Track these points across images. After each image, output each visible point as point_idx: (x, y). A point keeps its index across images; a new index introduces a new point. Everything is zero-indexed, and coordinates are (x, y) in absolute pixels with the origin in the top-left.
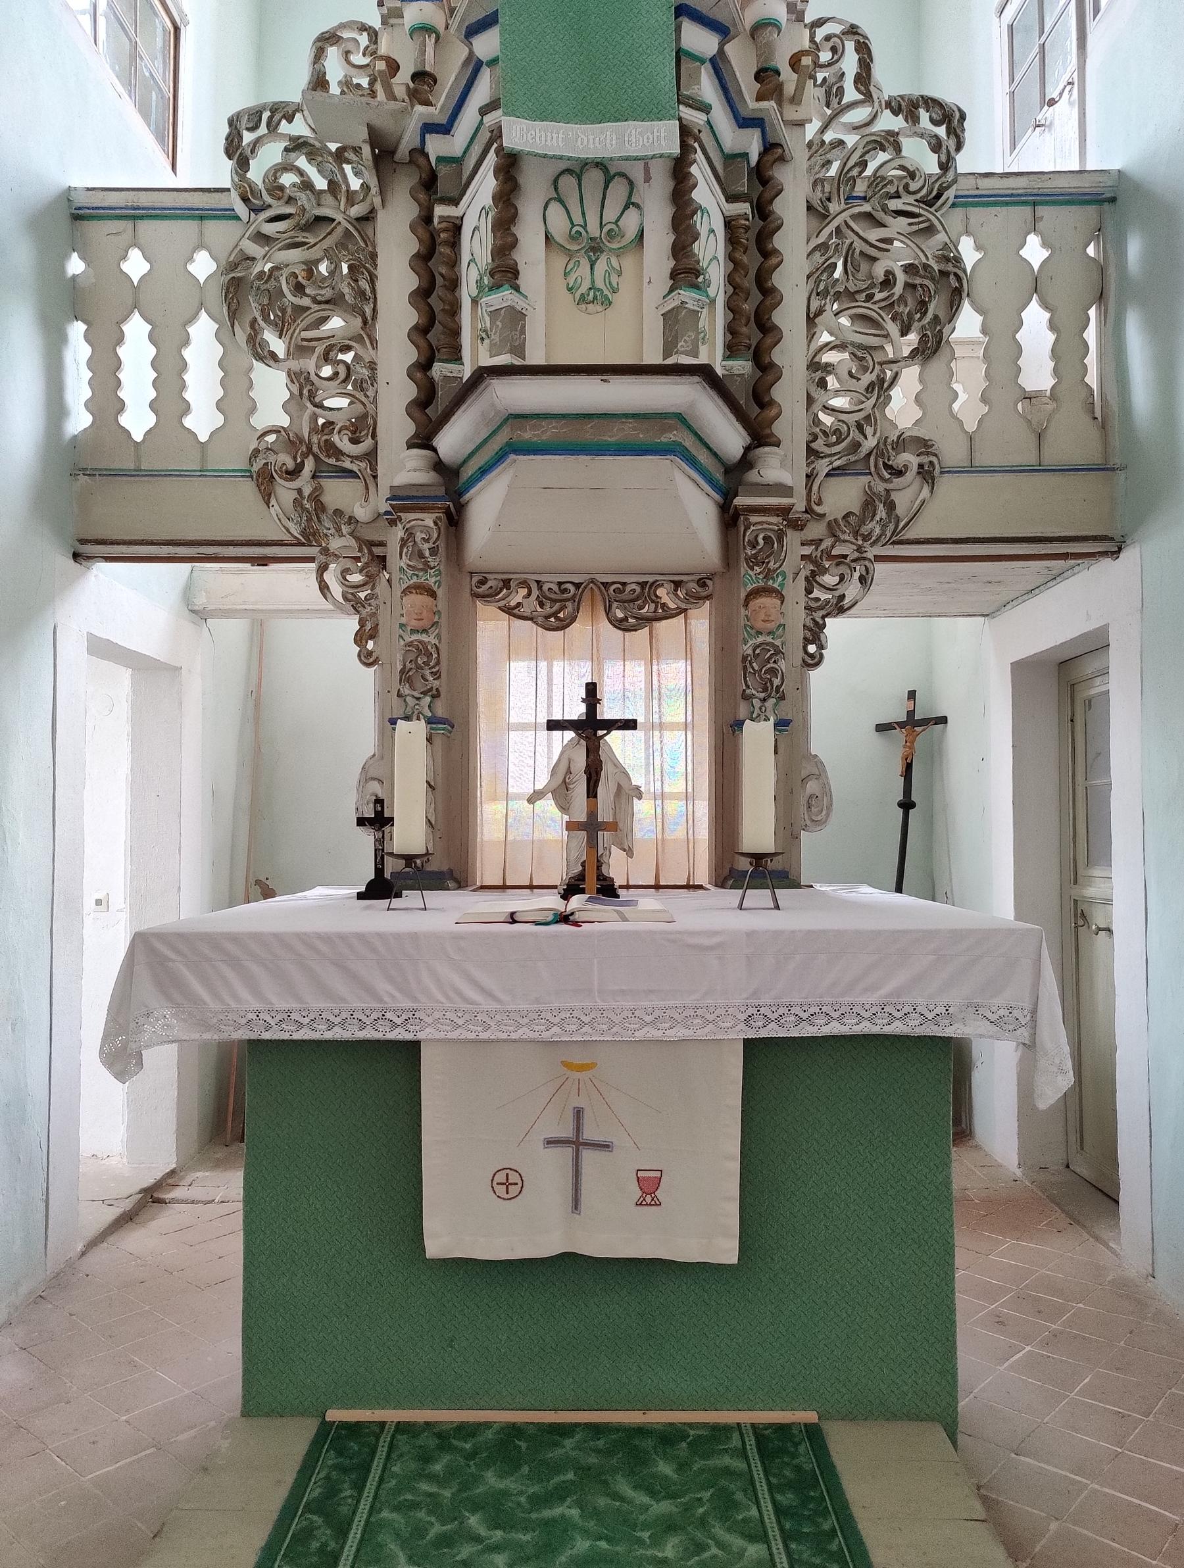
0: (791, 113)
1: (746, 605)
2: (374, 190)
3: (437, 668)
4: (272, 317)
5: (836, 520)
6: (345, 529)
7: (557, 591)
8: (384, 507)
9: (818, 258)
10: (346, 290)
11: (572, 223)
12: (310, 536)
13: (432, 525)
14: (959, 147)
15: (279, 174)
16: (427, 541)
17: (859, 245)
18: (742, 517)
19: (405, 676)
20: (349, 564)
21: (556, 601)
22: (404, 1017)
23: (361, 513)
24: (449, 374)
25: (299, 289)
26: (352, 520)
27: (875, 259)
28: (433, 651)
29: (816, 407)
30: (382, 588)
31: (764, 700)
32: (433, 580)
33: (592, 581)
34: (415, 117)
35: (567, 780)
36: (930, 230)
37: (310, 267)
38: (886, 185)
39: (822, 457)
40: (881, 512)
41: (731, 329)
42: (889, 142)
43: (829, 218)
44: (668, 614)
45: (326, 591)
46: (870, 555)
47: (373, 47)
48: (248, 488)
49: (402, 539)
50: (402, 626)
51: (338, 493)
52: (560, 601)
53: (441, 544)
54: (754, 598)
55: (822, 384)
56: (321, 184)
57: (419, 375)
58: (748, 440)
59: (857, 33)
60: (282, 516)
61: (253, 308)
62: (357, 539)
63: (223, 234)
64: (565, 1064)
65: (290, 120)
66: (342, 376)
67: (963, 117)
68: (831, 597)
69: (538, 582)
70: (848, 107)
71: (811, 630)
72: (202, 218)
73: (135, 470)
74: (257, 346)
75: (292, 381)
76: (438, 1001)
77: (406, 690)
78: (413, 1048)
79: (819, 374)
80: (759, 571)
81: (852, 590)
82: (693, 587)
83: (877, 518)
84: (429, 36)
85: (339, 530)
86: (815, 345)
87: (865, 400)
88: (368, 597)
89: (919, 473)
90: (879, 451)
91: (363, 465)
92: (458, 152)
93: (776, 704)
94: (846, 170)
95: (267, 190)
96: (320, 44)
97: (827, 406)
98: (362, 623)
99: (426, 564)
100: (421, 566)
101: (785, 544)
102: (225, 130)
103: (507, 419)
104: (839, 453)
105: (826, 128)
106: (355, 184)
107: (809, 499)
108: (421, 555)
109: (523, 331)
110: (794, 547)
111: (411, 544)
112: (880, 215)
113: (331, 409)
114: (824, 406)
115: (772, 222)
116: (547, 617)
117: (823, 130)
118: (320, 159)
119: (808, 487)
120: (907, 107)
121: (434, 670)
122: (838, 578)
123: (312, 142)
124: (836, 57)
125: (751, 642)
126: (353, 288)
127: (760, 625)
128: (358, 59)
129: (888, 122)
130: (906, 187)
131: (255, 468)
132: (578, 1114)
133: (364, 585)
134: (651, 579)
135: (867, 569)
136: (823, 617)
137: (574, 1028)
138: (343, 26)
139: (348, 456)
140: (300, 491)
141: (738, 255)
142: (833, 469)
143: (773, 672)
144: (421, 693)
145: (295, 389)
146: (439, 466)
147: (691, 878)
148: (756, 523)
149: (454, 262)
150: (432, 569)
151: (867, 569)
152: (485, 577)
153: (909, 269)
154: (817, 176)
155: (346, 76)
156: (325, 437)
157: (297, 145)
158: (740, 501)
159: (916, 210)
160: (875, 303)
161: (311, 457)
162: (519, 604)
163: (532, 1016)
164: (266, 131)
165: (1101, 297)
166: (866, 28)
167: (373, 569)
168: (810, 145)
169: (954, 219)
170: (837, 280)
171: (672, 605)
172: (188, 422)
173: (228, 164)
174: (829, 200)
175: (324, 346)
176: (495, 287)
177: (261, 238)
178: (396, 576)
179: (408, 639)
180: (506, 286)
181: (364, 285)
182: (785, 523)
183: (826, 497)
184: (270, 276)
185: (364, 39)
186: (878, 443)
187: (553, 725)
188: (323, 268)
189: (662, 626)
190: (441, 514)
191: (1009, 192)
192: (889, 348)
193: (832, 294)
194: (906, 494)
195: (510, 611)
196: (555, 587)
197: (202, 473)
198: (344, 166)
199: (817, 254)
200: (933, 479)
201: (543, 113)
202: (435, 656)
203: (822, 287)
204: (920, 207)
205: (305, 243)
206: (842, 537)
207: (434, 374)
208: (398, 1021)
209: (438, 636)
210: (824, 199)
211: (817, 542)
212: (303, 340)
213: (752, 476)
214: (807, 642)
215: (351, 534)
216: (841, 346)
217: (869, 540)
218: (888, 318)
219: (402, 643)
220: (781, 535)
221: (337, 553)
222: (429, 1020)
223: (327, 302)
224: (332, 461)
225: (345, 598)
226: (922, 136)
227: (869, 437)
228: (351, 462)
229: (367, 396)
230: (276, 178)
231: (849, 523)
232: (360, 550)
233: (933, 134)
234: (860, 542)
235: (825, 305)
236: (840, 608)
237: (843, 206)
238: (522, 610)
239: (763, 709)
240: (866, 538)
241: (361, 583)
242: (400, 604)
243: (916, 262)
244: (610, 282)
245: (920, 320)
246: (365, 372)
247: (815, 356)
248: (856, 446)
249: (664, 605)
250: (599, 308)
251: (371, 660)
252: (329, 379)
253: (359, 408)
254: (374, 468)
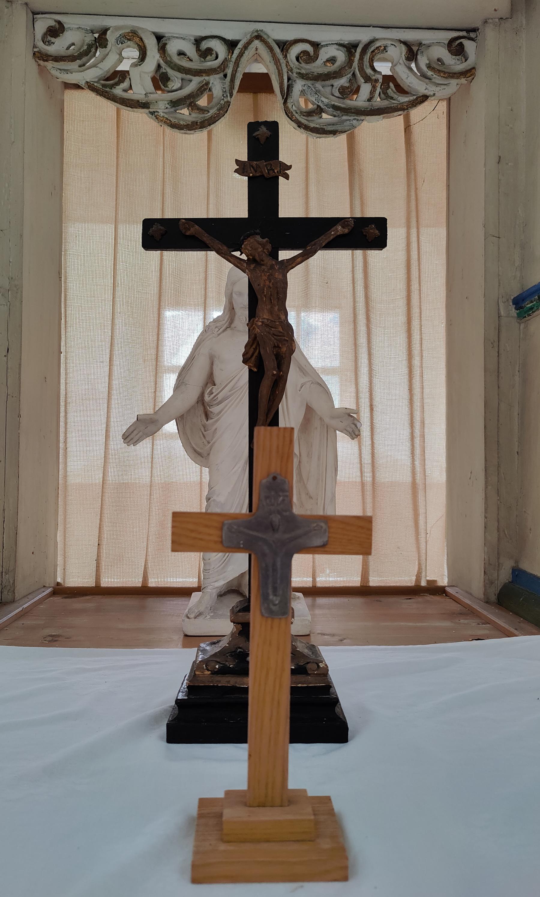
33: (259, 36)
35: (207, 398)
69: (159, 38)
116: (175, 104)
152: (59, 23)
196: (190, 50)
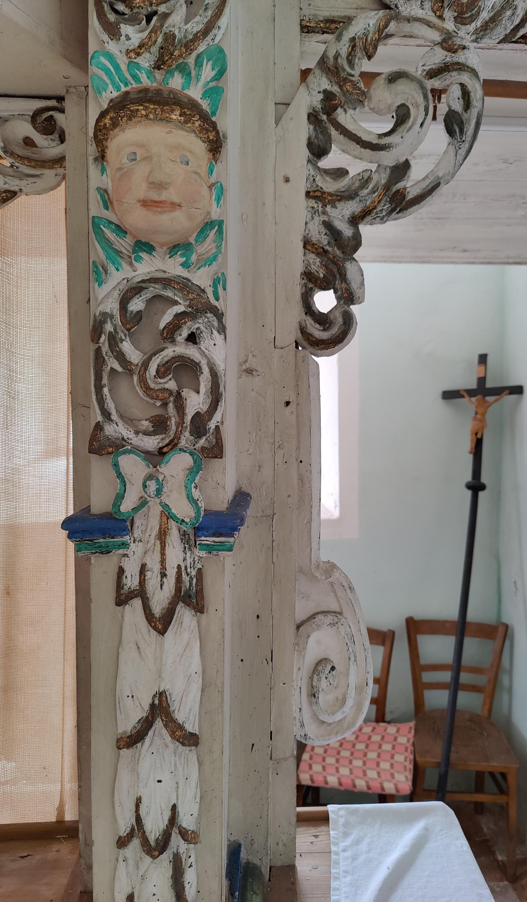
68: (373, 167)
71: (322, 253)
217: (473, 19)
234: (450, 25)
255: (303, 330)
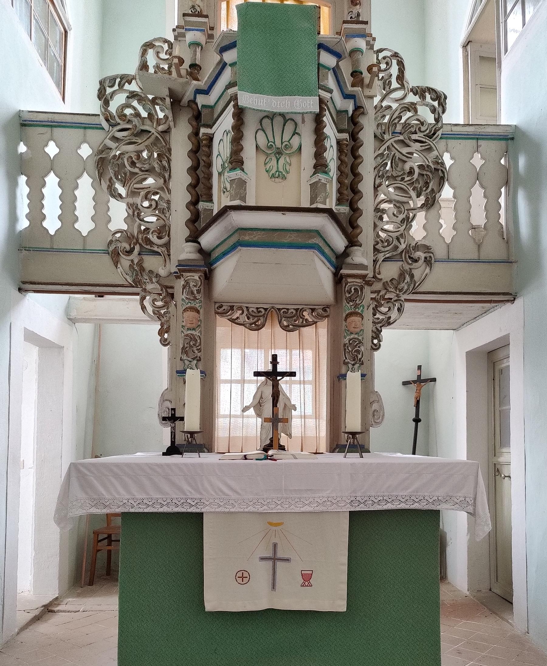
0: (367, 92)
1: (346, 320)
2: (171, 118)
3: (200, 347)
4: (120, 177)
5: (387, 282)
6: (154, 280)
7: (256, 312)
8: (174, 269)
9: (379, 160)
10: (156, 166)
11: (268, 140)
12: (137, 283)
13: (198, 279)
14: (444, 111)
15: (124, 108)
16: (195, 286)
17: (398, 155)
18: (344, 279)
19: (184, 350)
20: (156, 297)
21: (255, 317)
22: (196, 502)
23: (162, 272)
24: (207, 208)
25: (133, 164)
26: (158, 276)
27: (405, 162)
28: (198, 339)
29: (378, 229)
30: (172, 308)
31: (353, 365)
32: (198, 305)
34: (192, 86)
35: (261, 401)
36: (430, 149)
37: (139, 154)
38: (411, 127)
39: (381, 253)
40: (408, 279)
41: (339, 191)
42: (412, 107)
43: (384, 142)
44: (308, 324)
45: (144, 309)
46: (402, 299)
47: (170, 50)
48: (107, 259)
49: (183, 285)
50: (183, 326)
51: (151, 262)
52: (257, 317)
53: (202, 287)
54: (349, 317)
55: (381, 218)
56: (144, 114)
57: (192, 207)
58: (347, 243)
59: (397, 56)
60: (123, 273)
61: (111, 173)
62: (160, 285)
63: (96, 136)
64: (270, 524)
65: (130, 83)
66: (154, 206)
67: (446, 98)
69: (247, 307)
70: (394, 90)
71: (375, 333)
72: (85, 128)
73: (50, 249)
74: (112, 191)
75: (129, 208)
76: (212, 495)
77: (185, 357)
78: (200, 516)
79: (379, 214)
80: (352, 304)
81: (394, 314)
82: (320, 311)
83: (406, 281)
84: (198, 48)
85: (151, 280)
86: (378, 200)
87: (400, 227)
88: (165, 313)
89: (425, 261)
90: (407, 250)
91: (163, 249)
92: (212, 103)
93: (359, 367)
94: (392, 120)
95: (118, 116)
96: (144, 48)
97: (383, 229)
98: (162, 325)
99: (195, 297)
100: (192, 298)
101: (364, 292)
102: (98, 86)
103: (237, 230)
104: (388, 251)
105: (383, 100)
106: (161, 115)
107: (374, 272)
108: (192, 293)
109: (245, 190)
110: (368, 294)
111: (188, 287)
112: (407, 141)
113: (148, 222)
114: (381, 229)
115: (359, 143)
116: (251, 324)
117: (382, 101)
118: (144, 102)
119: (374, 265)
120: (421, 92)
121: (198, 348)
122: (387, 309)
123: (140, 94)
124: (388, 67)
125: (348, 337)
126: (160, 165)
127: (352, 329)
128: (163, 56)
129: (412, 98)
130: (419, 129)
131: (111, 248)
132: (275, 546)
133: (163, 307)
134: (300, 307)
135: (401, 305)
136: (381, 327)
137: (273, 506)
138: (156, 40)
139: (157, 245)
140: (132, 261)
141: (343, 157)
142: (385, 258)
143: (358, 352)
144: (192, 359)
145: (131, 212)
146: (201, 251)
147: (318, 449)
148: (351, 282)
149: (209, 155)
150: (197, 300)
151: (401, 305)
152: (221, 304)
153: (421, 167)
154: (379, 122)
155: (157, 64)
156: (145, 236)
157: (133, 95)
158: (344, 271)
159: (424, 140)
160: (405, 182)
161: (138, 245)
162: (238, 318)
163: (254, 501)
164: (118, 88)
165: (507, 183)
166: (402, 54)
167: (168, 299)
168: (376, 107)
169: (441, 145)
170: (388, 171)
171: (310, 320)
172: (77, 226)
173: (99, 103)
174: (384, 133)
175: (145, 192)
176: (233, 169)
177: (115, 139)
178: (180, 303)
179: (186, 333)
180: (238, 169)
181: (165, 163)
182: (364, 282)
183: (382, 271)
184: (119, 157)
185: (166, 47)
186: (406, 247)
187: (257, 374)
188: (145, 154)
189: (305, 330)
190: (202, 274)
191: (466, 133)
192: (411, 202)
193: (385, 177)
194: (419, 271)
195: (233, 321)
196: (255, 310)
197: (84, 251)
198: (156, 106)
199: (379, 158)
200: (431, 264)
201: (256, 89)
202: (199, 341)
203: (381, 174)
204: (426, 139)
205: (136, 143)
206: (390, 290)
207: (199, 207)
208: (193, 504)
209: (200, 332)
210: (382, 133)
211: (378, 292)
212: (135, 188)
213: (349, 260)
214: (373, 338)
215: (157, 282)
216: (390, 201)
217: (402, 291)
218: (411, 189)
219: (183, 335)
220: (362, 288)
221: (150, 291)
222: (207, 503)
223: (147, 171)
224: (148, 247)
225: (154, 313)
226: (427, 105)
227: (402, 243)
228: (158, 248)
229: (166, 217)
230: (122, 111)
231: (393, 283)
232: (162, 290)
233: (432, 105)
234: (398, 293)
235: (382, 181)
236: (388, 323)
237: (391, 136)
238: (239, 321)
239: (353, 369)
240: (400, 290)
241: (162, 306)
242: (182, 316)
243: (424, 164)
244: (286, 169)
245: (425, 190)
246: (165, 205)
247: (378, 205)
248: (396, 248)
249: (306, 320)
250: (281, 180)
251: (167, 343)
252: (148, 208)
253: (162, 222)
254: (168, 250)
255: (371, 347)
